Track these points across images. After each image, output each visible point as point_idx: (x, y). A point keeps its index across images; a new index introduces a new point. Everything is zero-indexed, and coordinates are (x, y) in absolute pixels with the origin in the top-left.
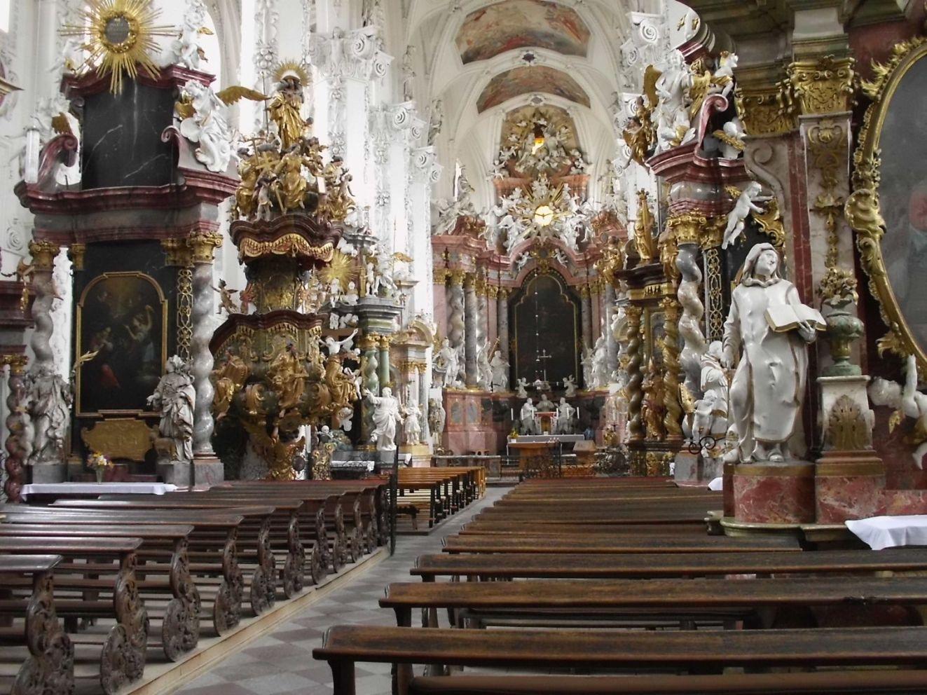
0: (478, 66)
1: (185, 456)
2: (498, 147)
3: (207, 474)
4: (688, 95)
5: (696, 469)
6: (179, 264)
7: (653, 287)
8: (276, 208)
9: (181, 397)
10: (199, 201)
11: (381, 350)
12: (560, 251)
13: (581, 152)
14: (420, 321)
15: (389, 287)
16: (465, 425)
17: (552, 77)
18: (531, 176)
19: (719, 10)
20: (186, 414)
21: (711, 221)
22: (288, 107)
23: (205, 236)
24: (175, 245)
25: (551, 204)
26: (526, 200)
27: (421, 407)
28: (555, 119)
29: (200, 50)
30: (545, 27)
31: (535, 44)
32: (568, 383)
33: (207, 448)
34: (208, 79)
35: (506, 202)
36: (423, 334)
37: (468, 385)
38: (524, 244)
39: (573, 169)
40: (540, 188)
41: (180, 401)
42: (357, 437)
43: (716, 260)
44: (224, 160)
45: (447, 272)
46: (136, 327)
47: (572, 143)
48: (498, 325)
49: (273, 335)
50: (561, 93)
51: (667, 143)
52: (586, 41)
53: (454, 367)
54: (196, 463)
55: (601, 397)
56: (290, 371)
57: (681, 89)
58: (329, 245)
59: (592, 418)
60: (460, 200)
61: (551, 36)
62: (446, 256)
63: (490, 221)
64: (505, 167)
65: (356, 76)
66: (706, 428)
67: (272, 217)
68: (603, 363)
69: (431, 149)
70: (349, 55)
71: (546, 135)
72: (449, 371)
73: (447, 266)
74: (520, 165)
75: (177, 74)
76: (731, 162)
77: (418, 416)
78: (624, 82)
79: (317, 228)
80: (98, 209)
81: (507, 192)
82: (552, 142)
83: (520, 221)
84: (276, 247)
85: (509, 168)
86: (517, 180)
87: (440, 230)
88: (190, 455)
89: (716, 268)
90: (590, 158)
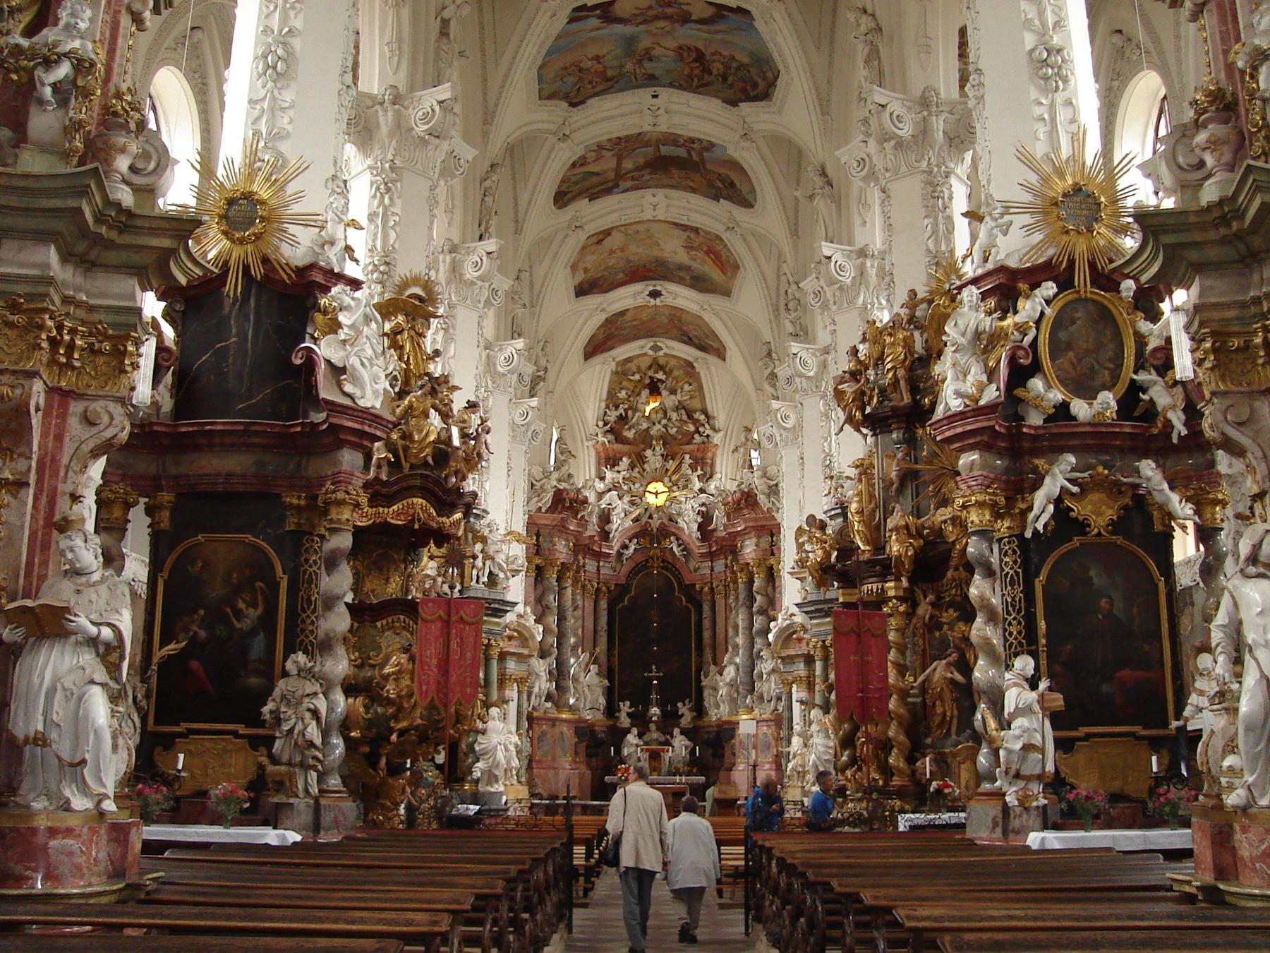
0: (593, 301)
1: (307, 791)
2: (603, 404)
3: (336, 817)
4: (984, 343)
5: (1000, 820)
6: (304, 528)
7: (875, 586)
8: (395, 466)
9: (309, 710)
10: (341, 444)
11: (488, 659)
12: (678, 539)
13: (707, 416)
14: (522, 621)
15: (502, 575)
16: (554, 760)
17: (680, 321)
19: (1182, 231)
20: (313, 733)
21: (1010, 501)
22: (413, 333)
23: (348, 493)
24: (302, 502)
25: (666, 479)
26: (635, 473)
27: (519, 735)
28: (676, 373)
29: (348, 249)
30: (683, 257)
31: (665, 278)
32: (684, 709)
33: (335, 782)
34: (355, 284)
36: (526, 639)
37: (558, 706)
38: (630, 528)
39: (696, 436)
40: (654, 458)
41: (308, 715)
42: (455, 772)
43: (1014, 552)
44: (375, 392)
45: (538, 561)
46: (241, 610)
47: (696, 404)
48: (595, 631)
49: (383, 631)
50: (689, 341)
51: (959, 401)
52: (734, 276)
53: (543, 684)
54: (323, 802)
55: (727, 731)
56: (405, 682)
57: (978, 335)
58: (458, 516)
59: (713, 755)
60: (557, 468)
61: (689, 269)
62: (537, 540)
63: (592, 497)
64: (611, 431)
65: (469, 301)
66: (1014, 767)
67: (390, 474)
68: (731, 685)
69: (534, 402)
70: (461, 275)
71: (664, 393)
72: (536, 690)
73: (537, 553)
74: (629, 429)
75: (319, 278)
76: (1036, 428)
77: (517, 746)
78: (790, 328)
79: (448, 491)
80: (197, 448)
81: (611, 461)
82: (671, 401)
83: (626, 499)
84: (393, 514)
85: (615, 431)
86: (626, 448)
87: (533, 507)
88: (314, 790)
89: (1015, 562)
90: (720, 422)
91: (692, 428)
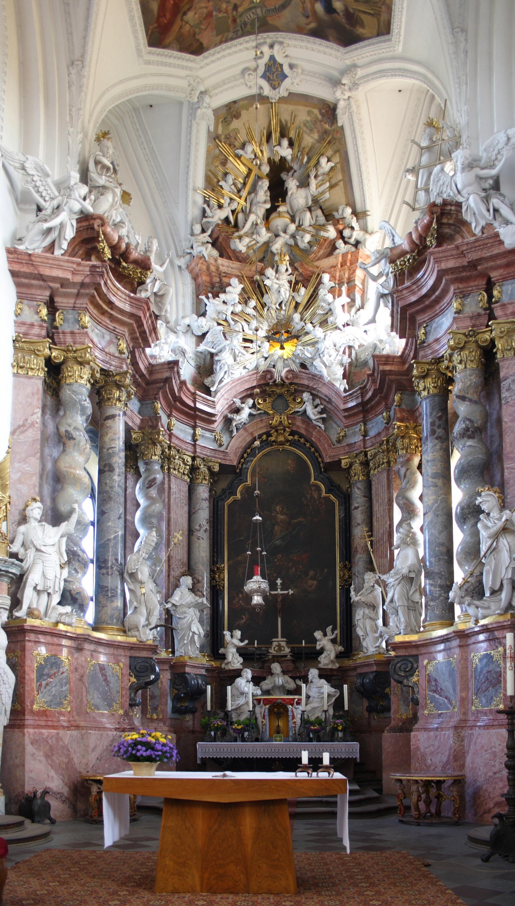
18: (261, 261)
25: (297, 317)
28: (309, 140)
35: (213, 305)
39: (340, 243)
40: (279, 283)
71: (292, 184)
81: (217, 288)
85: (220, 243)
91: (331, 233)
